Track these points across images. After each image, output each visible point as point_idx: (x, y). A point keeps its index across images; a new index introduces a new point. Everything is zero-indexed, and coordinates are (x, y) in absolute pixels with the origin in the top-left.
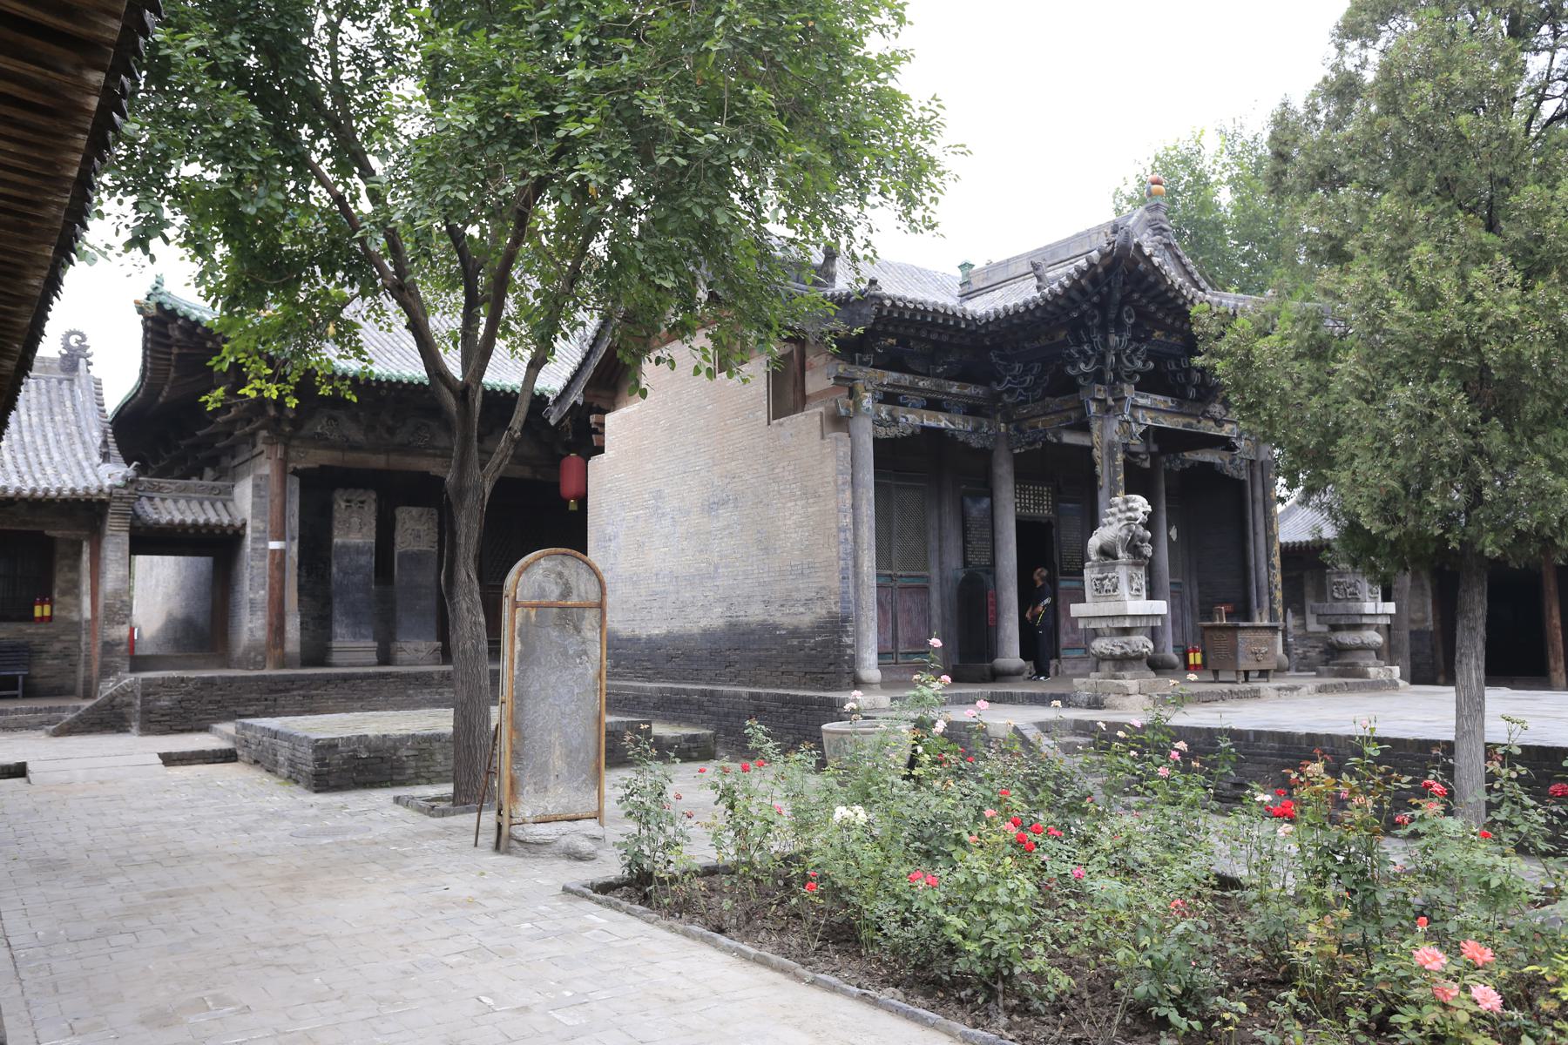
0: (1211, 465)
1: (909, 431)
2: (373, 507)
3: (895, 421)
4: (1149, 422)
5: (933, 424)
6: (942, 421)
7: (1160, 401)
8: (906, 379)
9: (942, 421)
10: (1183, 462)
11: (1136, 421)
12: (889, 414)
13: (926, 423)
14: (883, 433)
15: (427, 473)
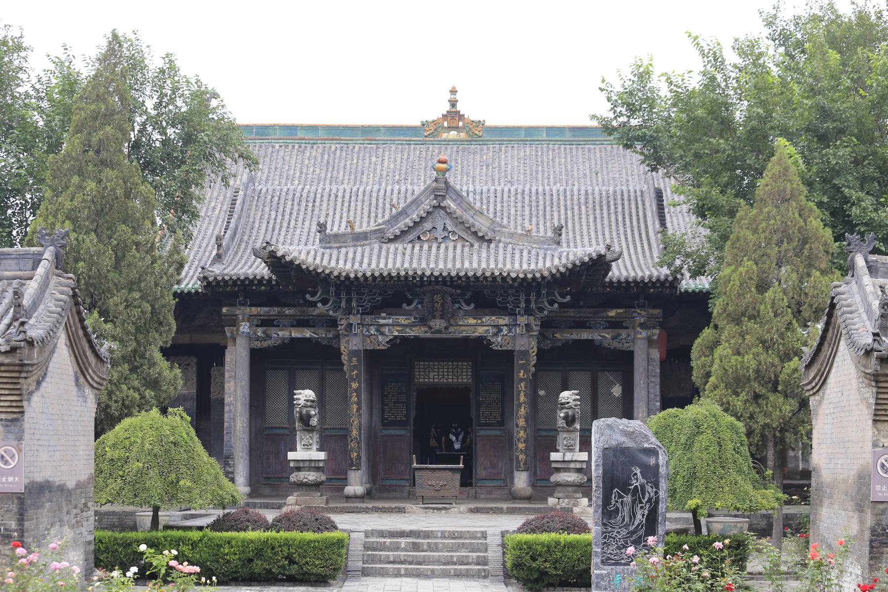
0: (590, 342)
1: (279, 342)
2: (195, 368)
3: (269, 337)
4: (396, 334)
5: (299, 335)
6: (308, 333)
7: (402, 320)
8: (275, 310)
9: (308, 333)
10: (555, 340)
11: (382, 334)
12: (264, 333)
13: (293, 335)
14: (258, 345)
15: (219, 344)
